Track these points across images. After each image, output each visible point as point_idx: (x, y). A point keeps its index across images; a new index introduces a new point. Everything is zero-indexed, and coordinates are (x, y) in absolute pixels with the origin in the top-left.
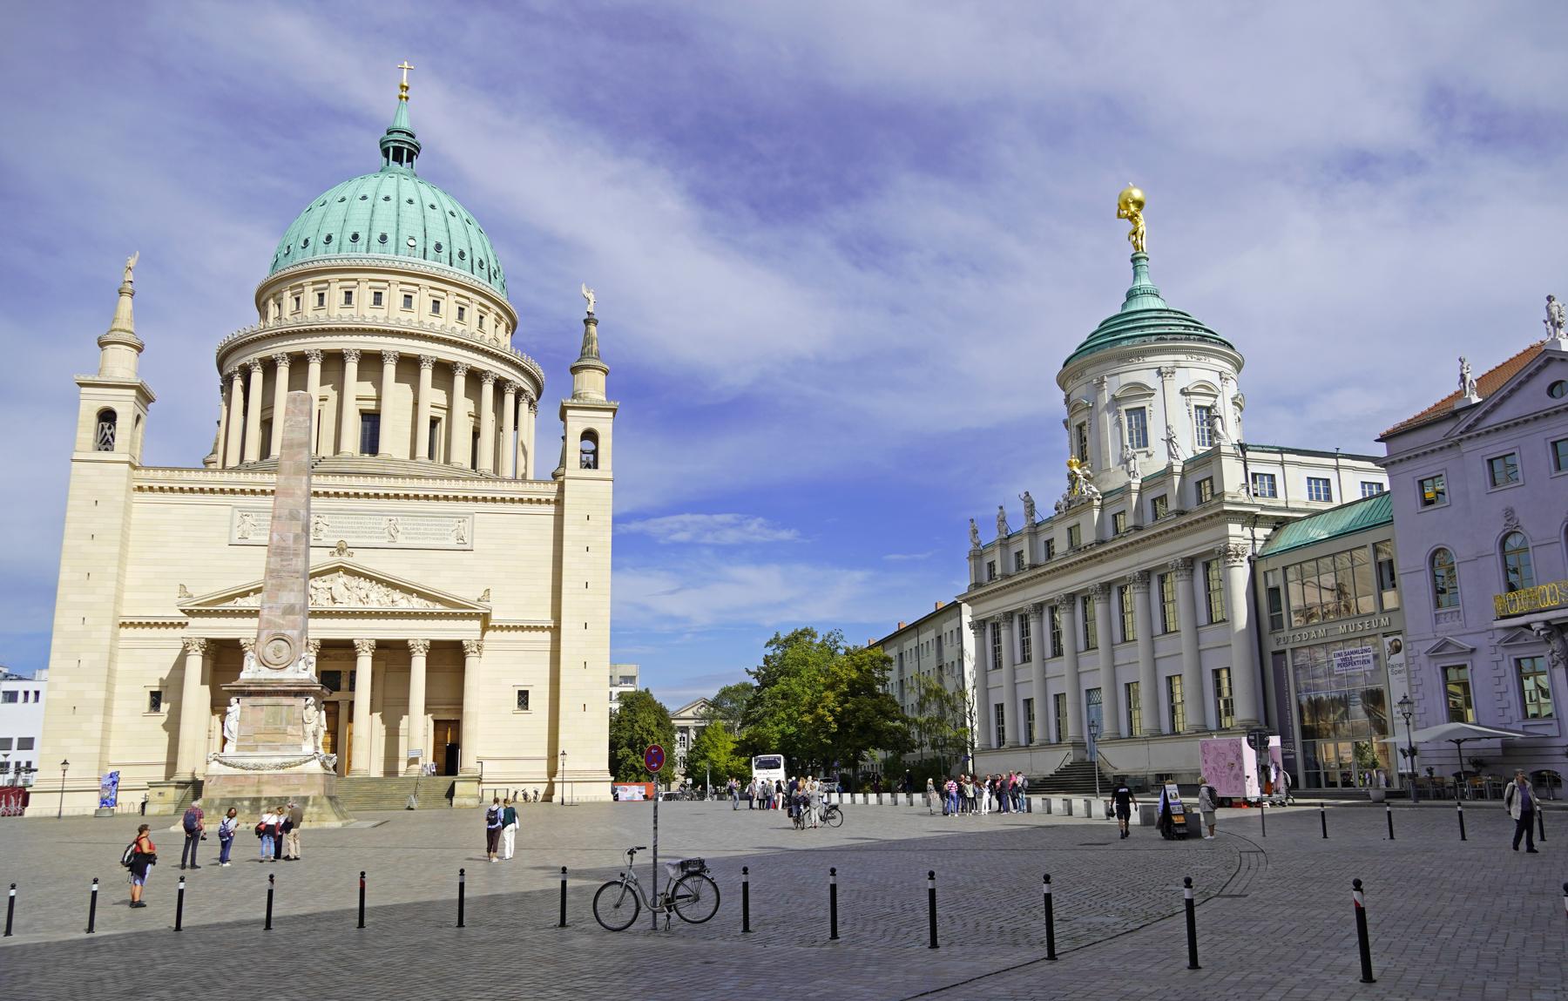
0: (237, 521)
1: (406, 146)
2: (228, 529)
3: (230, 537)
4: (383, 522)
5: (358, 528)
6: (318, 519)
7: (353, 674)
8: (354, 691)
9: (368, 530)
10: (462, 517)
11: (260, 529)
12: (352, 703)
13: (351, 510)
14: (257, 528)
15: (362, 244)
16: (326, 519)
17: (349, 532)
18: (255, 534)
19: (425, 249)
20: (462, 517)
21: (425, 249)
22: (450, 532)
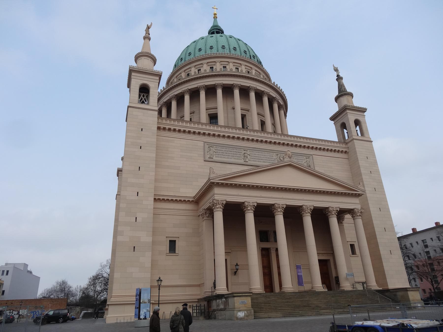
0: (207, 149)
1: (221, 32)
2: (202, 153)
3: (204, 157)
4: (274, 156)
5: (263, 157)
6: (245, 151)
7: (275, 233)
8: (277, 242)
9: (268, 159)
10: (308, 156)
11: (218, 154)
12: (277, 250)
13: (259, 149)
14: (217, 153)
15: (227, 50)
16: (248, 152)
17: (260, 159)
18: (216, 157)
19: (250, 56)
20: (308, 156)
21: (250, 56)
22: (304, 163)
